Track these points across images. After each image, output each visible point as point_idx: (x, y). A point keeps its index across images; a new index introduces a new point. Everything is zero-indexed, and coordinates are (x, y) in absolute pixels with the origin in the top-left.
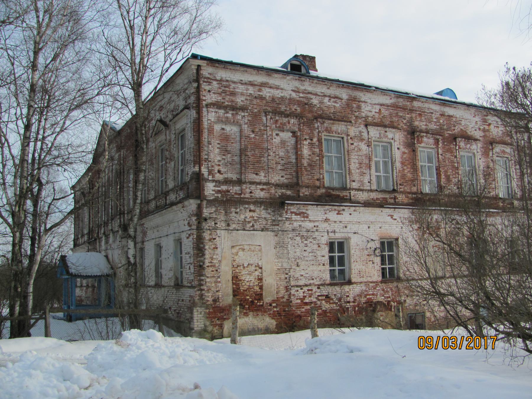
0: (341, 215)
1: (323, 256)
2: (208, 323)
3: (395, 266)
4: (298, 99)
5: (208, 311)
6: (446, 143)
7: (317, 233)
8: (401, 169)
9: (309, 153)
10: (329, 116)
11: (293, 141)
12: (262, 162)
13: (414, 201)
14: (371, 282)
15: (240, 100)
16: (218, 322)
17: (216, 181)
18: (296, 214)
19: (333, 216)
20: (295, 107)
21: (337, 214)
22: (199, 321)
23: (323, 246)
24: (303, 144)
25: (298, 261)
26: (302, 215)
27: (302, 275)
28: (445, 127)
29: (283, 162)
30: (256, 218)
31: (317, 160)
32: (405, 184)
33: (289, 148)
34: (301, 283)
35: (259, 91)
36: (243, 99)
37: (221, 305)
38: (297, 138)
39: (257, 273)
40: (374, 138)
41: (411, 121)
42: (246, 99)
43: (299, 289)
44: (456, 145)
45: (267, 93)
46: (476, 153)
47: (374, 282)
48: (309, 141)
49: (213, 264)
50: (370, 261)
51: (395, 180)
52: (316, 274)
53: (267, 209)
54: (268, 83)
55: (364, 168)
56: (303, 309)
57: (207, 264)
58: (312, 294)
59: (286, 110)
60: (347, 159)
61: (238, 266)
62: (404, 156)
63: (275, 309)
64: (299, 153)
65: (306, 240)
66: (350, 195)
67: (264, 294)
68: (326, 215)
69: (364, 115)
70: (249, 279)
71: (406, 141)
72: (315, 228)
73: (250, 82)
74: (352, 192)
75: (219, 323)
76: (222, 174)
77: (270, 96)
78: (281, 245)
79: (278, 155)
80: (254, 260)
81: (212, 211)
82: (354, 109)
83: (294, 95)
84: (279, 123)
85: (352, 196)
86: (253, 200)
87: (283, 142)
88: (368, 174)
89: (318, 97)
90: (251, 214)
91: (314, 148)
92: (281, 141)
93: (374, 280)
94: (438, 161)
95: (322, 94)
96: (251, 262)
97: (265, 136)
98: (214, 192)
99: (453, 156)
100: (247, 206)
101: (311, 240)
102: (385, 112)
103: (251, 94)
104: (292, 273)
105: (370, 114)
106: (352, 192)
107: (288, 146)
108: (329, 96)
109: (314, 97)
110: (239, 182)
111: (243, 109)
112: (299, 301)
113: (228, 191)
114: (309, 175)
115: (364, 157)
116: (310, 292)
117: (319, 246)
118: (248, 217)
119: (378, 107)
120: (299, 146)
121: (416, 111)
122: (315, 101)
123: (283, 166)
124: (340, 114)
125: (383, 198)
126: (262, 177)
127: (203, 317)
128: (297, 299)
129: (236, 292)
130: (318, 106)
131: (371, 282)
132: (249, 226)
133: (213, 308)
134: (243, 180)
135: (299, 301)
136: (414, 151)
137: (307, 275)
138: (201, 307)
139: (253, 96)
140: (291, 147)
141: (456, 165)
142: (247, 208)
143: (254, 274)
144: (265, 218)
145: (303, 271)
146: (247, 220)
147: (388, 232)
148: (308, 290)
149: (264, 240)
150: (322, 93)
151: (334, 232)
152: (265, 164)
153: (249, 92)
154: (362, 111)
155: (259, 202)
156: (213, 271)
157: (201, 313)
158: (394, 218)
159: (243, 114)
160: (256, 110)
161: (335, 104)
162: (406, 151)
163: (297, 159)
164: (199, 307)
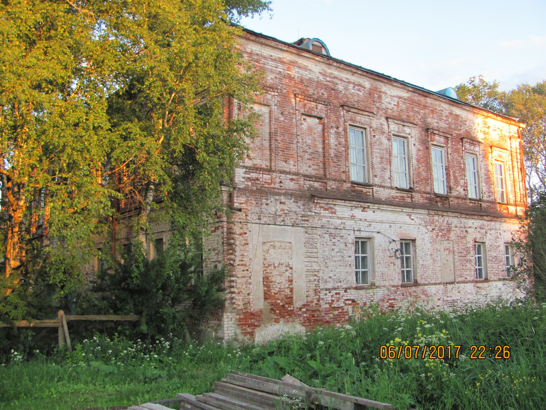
0: (366, 213)
1: (350, 257)
2: (239, 331)
3: (411, 269)
4: (325, 83)
5: (238, 317)
6: (454, 143)
7: (344, 231)
8: (417, 167)
9: (336, 143)
10: (353, 105)
11: (320, 127)
12: (292, 149)
13: (428, 201)
14: (393, 286)
15: (270, 78)
16: (249, 330)
17: (246, 167)
18: (325, 209)
19: (358, 213)
20: (322, 91)
21: (362, 211)
22: (230, 328)
23: (349, 245)
24: (330, 133)
25: (326, 261)
26: (330, 210)
27: (330, 277)
28: (453, 126)
29: (309, 151)
30: (286, 212)
31: (343, 151)
32: (421, 183)
33: (316, 136)
34: (329, 286)
35: (288, 70)
36: (273, 77)
37: (252, 310)
38: (324, 126)
39: (287, 274)
40: (393, 132)
41: (424, 118)
42: (276, 78)
43: (327, 292)
44: (462, 146)
45: (294, 72)
46: (478, 155)
47: (395, 286)
48: (335, 129)
49: (244, 263)
50: (391, 263)
51: (412, 178)
52: (343, 277)
53: (297, 202)
54: (296, 62)
55: (385, 163)
56: (331, 315)
57: (237, 262)
58: (339, 298)
59: (314, 94)
60: (370, 152)
61: (269, 265)
62: (420, 153)
63: (305, 315)
64: (326, 142)
65: (334, 238)
66: (373, 191)
67: (294, 298)
68: (352, 212)
69: (384, 106)
70: (279, 281)
71: (420, 137)
72: (342, 226)
73: (280, 58)
74: (375, 188)
75: (250, 331)
76: (251, 159)
77: (298, 77)
78: (310, 244)
79: (306, 142)
80: (285, 259)
81: (243, 202)
82: (375, 99)
83: (321, 78)
84: (307, 107)
85: (374, 192)
86: (283, 191)
87: (310, 129)
88: (389, 170)
89: (343, 83)
90: (282, 206)
91: (340, 138)
92: (308, 127)
93: (396, 284)
94: (448, 161)
95: (347, 80)
96: (282, 261)
97: (294, 120)
98: (244, 180)
99: (459, 157)
100: (277, 197)
101: (338, 238)
102: (403, 107)
103: (280, 72)
104: (320, 274)
105: (389, 106)
106: (375, 188)
107: (315, 133)
108: (354, 83)
109: (340, 82)
110: (269, 170)
111: (272, 88)
112: (328, 306)
113: (257, 179)
114: (335, 167)
115: (384, 152)
116: (338, 296)
117: (346, 245)
118: (279, 210)
119: (396, 99)
120: (326, 134)
121: (429, 107)
122: (340, 87)
123: (311, 155)
124: (363, 103)
125: (402, 197)
126: (291, 166)
127: (233, 324)
128: (326, 303)
129: (267, 296)
130: (343, 92)
131: (393, 286)
132: (280, 219)
133: (244, 313)
134: (273, 168)
135: (328, 306)
136: (427, 148)
137: (335, 277)
138: (231, 312)
139: (282, 75)
140: (317, 134)
141: (462, 166)
142: (278, 200)
143: (285, 275)
144: (295, 212)
145: (331, 273)
146: (278, 213)
147: (407, 232)
148: (336, 294)
149: (294, 236)
150: (347, 79)
151: (359, 230)
152: (294, 151)
153: (279, 70)
154: (383, 102)
155: (289, 194)
156: (243, 271)
157: (231, 320)
158: (412, 217)
159: (273, 93)
160: (285, 91)
161: (359, 92)
162: (421, 148)
163: (324, 148)
164: (230, 313)
